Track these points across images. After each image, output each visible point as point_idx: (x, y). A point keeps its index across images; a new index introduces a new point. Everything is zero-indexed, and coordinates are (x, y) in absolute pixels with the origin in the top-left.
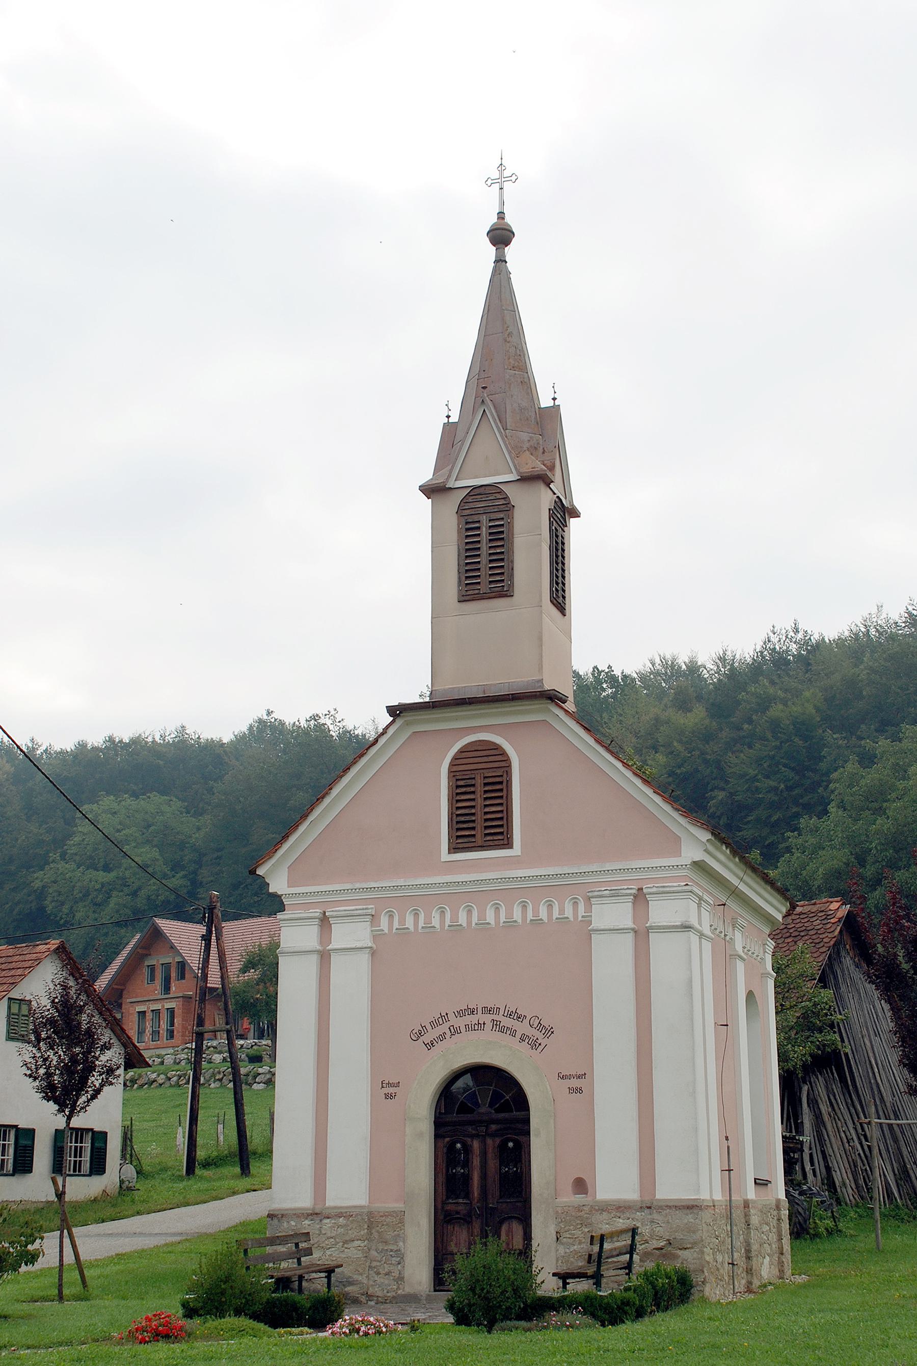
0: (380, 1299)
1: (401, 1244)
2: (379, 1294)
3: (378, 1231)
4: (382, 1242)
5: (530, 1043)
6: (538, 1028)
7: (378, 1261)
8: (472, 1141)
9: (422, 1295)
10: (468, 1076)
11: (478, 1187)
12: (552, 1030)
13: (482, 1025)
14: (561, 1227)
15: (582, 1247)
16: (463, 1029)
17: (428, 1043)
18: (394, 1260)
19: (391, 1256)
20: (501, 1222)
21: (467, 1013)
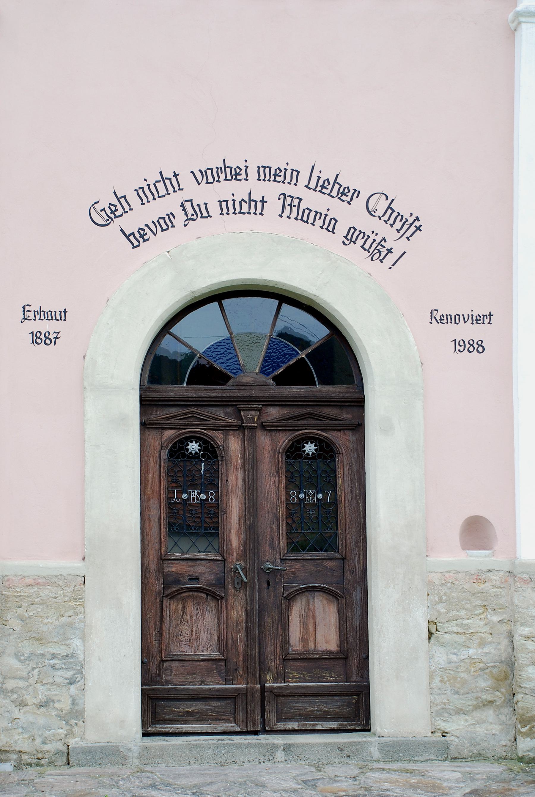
0: (25, 757)
1: (77, 643)
2: (24, 745)
3: (21, 618)
4: (31, 638)
5: (367, 246)
6: (386, 217)
7: (21, 678)
8: (226, 439)
9: (129, 749)
10: (323, 332)
11: (240, 529)
12: (417, 224)
13: (259, 205)
14: (438, 611)
15: (486, 650)
16: (214, 209)
17: (133, 234)
18: (60, 676)
19: (53, 667)
20: (290, 599)
21: (222, 176)
